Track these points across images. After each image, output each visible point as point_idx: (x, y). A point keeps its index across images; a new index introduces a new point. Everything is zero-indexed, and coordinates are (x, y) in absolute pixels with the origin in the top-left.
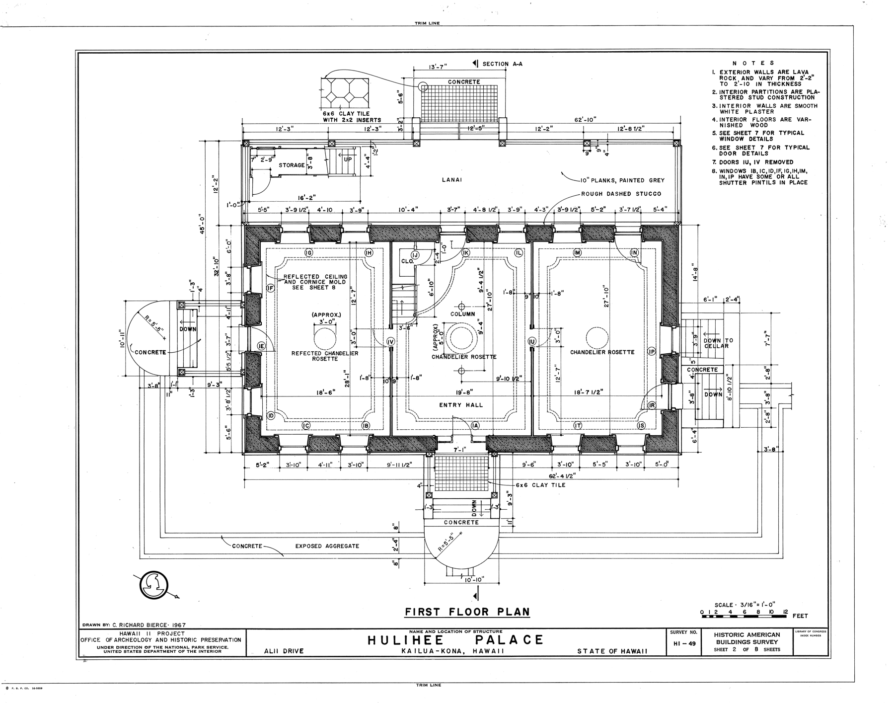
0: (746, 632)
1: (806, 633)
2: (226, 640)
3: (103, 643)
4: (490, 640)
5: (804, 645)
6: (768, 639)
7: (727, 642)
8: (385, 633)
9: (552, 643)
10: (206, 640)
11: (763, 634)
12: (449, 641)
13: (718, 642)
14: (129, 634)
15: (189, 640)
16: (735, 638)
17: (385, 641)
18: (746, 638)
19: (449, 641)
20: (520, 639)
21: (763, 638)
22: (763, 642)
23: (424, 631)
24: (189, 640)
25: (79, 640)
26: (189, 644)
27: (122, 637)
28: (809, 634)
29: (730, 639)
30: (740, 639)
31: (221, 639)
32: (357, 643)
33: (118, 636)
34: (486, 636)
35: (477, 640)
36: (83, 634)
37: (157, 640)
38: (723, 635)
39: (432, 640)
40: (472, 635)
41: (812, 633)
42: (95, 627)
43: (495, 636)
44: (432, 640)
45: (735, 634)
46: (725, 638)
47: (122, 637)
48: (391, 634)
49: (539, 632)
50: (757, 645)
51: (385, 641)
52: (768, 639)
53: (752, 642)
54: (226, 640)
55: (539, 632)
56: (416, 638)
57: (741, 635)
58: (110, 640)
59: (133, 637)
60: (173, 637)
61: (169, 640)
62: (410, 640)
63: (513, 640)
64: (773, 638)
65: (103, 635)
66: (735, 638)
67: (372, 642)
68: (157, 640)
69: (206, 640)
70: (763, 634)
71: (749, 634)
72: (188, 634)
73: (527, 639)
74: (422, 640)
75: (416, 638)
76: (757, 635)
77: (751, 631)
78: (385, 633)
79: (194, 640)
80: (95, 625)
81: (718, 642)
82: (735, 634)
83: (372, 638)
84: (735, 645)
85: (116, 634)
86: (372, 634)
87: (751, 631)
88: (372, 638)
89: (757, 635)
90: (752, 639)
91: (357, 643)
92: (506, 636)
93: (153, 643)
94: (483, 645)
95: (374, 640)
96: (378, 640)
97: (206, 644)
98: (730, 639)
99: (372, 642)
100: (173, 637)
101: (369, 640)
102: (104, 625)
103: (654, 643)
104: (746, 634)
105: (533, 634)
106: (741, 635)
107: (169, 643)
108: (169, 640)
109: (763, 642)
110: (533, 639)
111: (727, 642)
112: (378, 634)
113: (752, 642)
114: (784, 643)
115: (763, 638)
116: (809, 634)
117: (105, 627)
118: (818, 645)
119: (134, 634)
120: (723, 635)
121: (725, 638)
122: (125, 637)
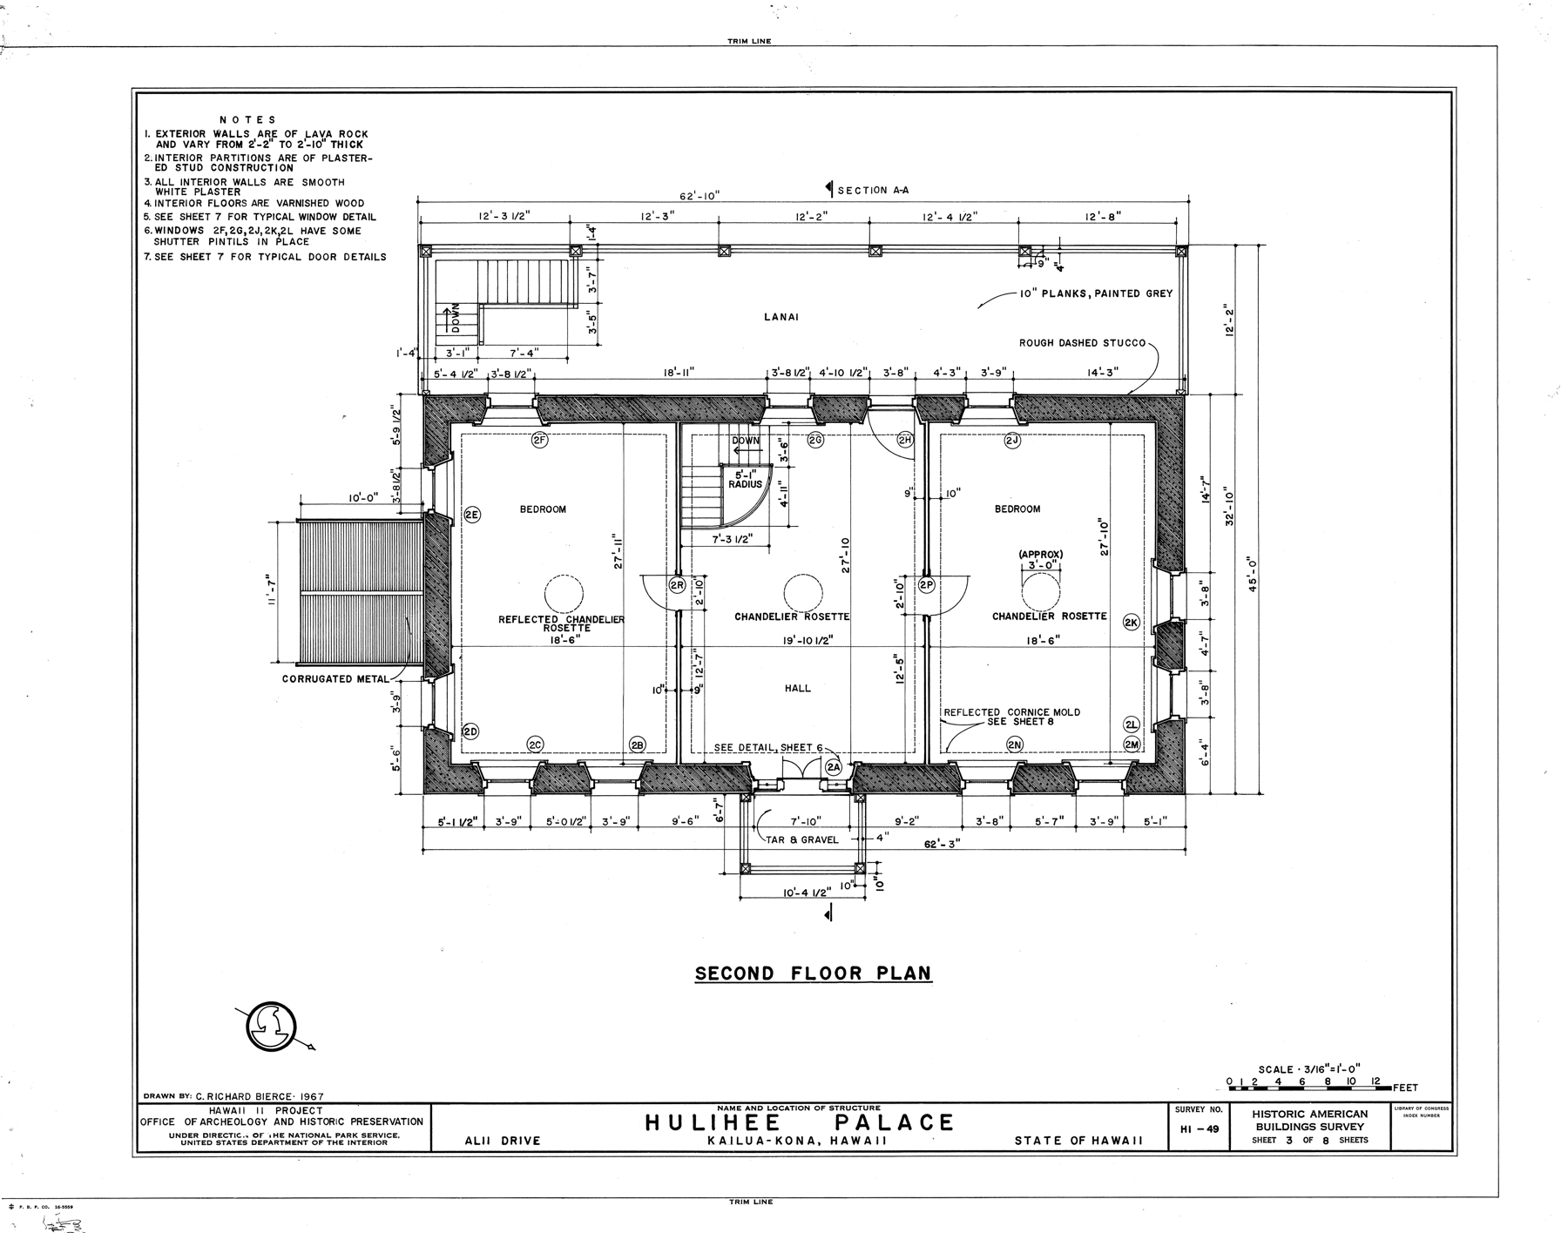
1: (1414, 1111)
2: (397, 1122)
3: (180, 1127)
4: (863, 1123)
5: (1410, 1131)
6: (1346, 1121)
7: (1274, 1127)
8: (676, 1110)
9: (970, 1128)
11: (1338, 1113)
12: (789, 1123)
14: (226, 1111)
15: (331, 1121)
16: (1289, 1120)
17: (676, 1124)
18: (1308, 1120)
20: (915, 1122)
23: (744, 1107)
24: (331, 1121)
25: (138, 1122)
26: (332, 1130)
27: (213, 1116)
28: (1419, 1113)
29: (1279, 1121)
30: (1298, 1121)
31: (386, 1121)
32: (627, 1129)
34: (854, 1117)
35: (838, 1123)
36: (145, 1112)
38: (1267, 1114)
39: (761, 1121)
40: (829, 1116)
41: (1423, 1111)
42: (166, 1099)
43: (872, 1117)
44: (761, 1121)
45: (1289, 1113)
46: (1271, 1120)
47: (213, 1116)
48: (687, 1112)
49: (946, 1109)
50: (1327, 1133)
51: (676, 1124)
52: (1346, 1121)
53: (1318, 1127)
54: (397, 1122)
55: (946, 1109)
56: (731, 1118)
57: (1298, 1114)
58: (193, 1121)
59: (234, 1116)
60: (302, 1116)
62: (720, 1122)
63: (905, 1123)
65: (180, 1113)
66: (1289, 1120)
67: (652, 1126)
68: (277, 1122)
70: (1338, 1113)
71: (1313, 1114)
72: (327, 1112)
73: (927, 1122)
74: (742, 1122)
75: (731, 1118)
76: (1328, 1114)
77: (1317, 1108)
78: (676, 1110)
79: (340, 1121)
80: (165, 1096)
82: (1289, 1113)
83: (652, 1118)
85: (203, 1112)
86: (652, 1111)
87: (1317, 1108)
88: (652, 1118)
89: (1328, 1114)
90: (1318, 1121)
91: (627, 1129)
92: (892, 1116)
93: (268, 1130)
94: (848, 1130)
95: (656, 1122)
96: (664, 1122)
97: (360, 1129)
98: (1279, 1121)
99: (652, 1126)
101: (648, 1122)
102: (182, 1096)
103: (1148, 1126)
104: (1308, 1113)
105: (936, 1111)
106: (1298, 1114)
107: (297, 1128)
109: (1338, 1126)
110: (936, 1122)
111: (1274, 1127)
112: (664, 1112)
113: (1318, 1127)
114: (1375, 1128)
116: (1419, 1113)
117: (184, 1100)
118: (1434, 1132)
120: (1267, 1114)
121: (1271, 1120)
122: (218, 1116)
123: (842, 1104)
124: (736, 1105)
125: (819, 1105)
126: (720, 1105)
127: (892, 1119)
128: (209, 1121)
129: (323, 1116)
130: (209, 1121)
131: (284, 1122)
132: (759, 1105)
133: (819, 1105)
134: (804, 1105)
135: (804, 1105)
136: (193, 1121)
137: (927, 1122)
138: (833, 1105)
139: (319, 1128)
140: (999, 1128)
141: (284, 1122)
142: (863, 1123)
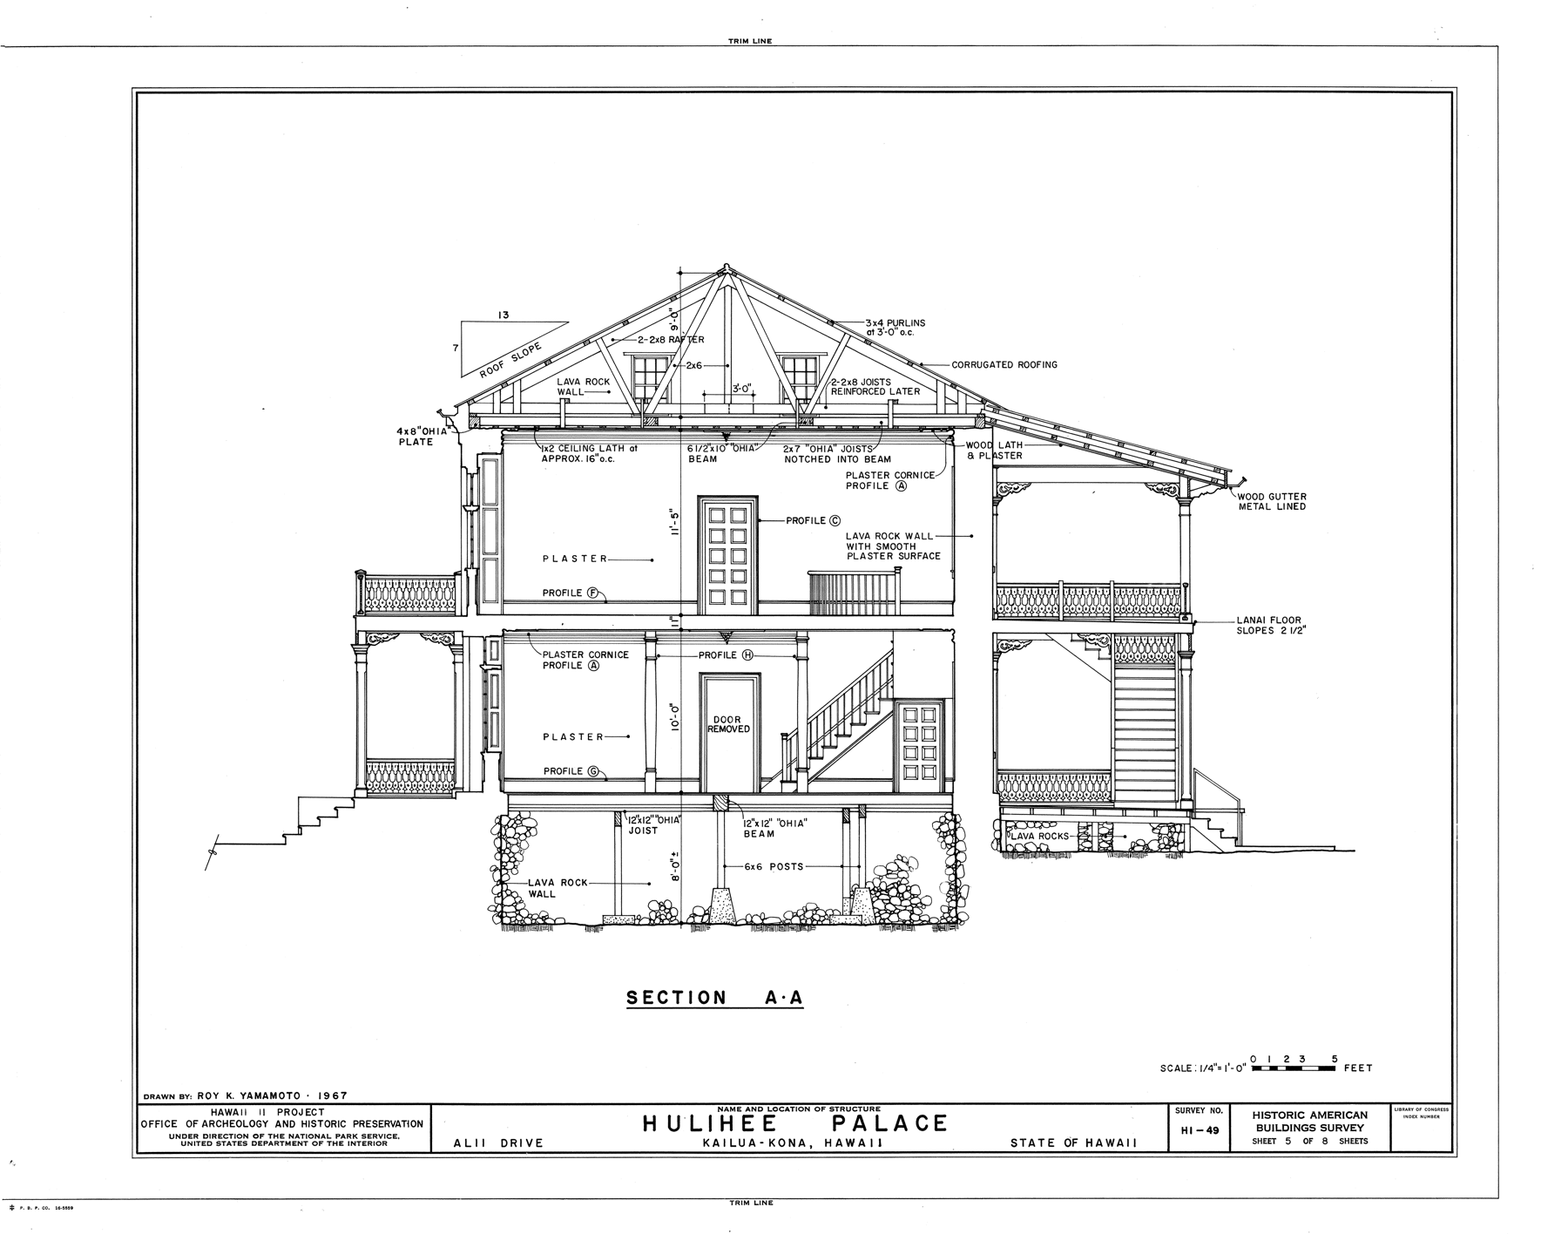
0: (1308, 1110)
1: (1414, 1113)
2: (397, 1124)
3: (182, 1129)
4: (860, 1124)
5: (1410, 1133)
6: (1346, 1122)
7: (1274, 1128)
8: (674, 1111)
10: (361, 1123)
11: (1338, 1114)
12: (786, 1125)
13: (1260, 1128)
14: (229, 1113)
15: (333, 1123)
16: (1289, 1121)
17: (674, 1126)
18: (1308, 1121)
19: (786, 1125)
21: (1338, 1121)
22: (1338, 1127)
23: (744, 1108)
24: (333, 1123)
25: (137, 1124)
26: (332, 1131)
27: (215, 1118)
28: (1419, 1114)
29: (1279, 1122)
30: (1298, 1122)
31: (387, 1123)
32: (624, 1129)
33: (209, 1118)
34: (851, 1117)
35: (835, 1123)
36: (146, 1113)
37: (278, 1124)
38: (1267, 1115)
39: (757, 1121)
40: (828, 1115)
41: (1423, 1112)
42: (166, 1100)
43: (869, 1118)
44: (757, 1121)
45: (1289, 1115)
46: (1271, 1121)
47: (215, 1118)
48: (685, 1112)
50: (1327, 1134)
51: (674, 1126)
52: (1346, 1122)
53: (1318, 1128)
54: (397, 1124)
56: (727, 1119)
57: (1298, 1115)
58: (195, 1123)
59: (236, 1118)
60: (304, 1118)
61: (298, 1124)
63: (901, 1123)
64: (1356, 1121)
65: (182, 1114)
66: (1289, 1121)
67: (650, 1127)
68: (278, 1124)
69: (361, 1123)
70: (1338, 1114)
71: (1313, 1115)
72: (331, 1113)
74: (738, 1123)
75: (727, 1119)
76: (1328, 1115)
77: (1317, 1109)
78: (674, 1111)
79: (341, 1124)
80: (165, 1097)
81: (1260, 1128)
82: (1289, 1115)
83: (650, 1119)
84: (1288, 1134)
85: (204, 1113)
86: (650, 1112)
87: (1317, 1109)
88: (650, 1119)
89: (1328, 1115)
90: (1318, 1122)
91: (624, 1129)
92: (888, 1117)
93: (271, 1128)
94: (845, 1131)
95: (654, 1123)
96: (662, 1123)
97: (360, 1131)
98: (1279, 1122)
99: (650, 1127)
100: (304, 1118)
101: (646, 1123)
102: (182, 1097)
103: (1147, 1129)
104: (1308, 1114)
105: (931, 1112)
106: (1298, 1115)
107: (298, 1130)
108: (298, 1124)
109: (1338, 1127)
111: (1274, 1128)
113: (1318, 1128)
114: (1375, 1130)
115: (1338, 1121)
116: (1419, 1114)
117: (183, 1101)
118: (1434, 1133)
119: (236, 1113)
120: (1267, 1115)
121: (1271, 1121)
122: (221, 1118)
123: (842, 1105)
124: (736, 1106)
125: (820, 1106)
126: (721, 1106)
128: (212, 1123)
129: (324, 1118)
130: (212, 1123)
131: (286, 1124)
132: (758, 1106)
133: (820, 1106)
134: (804, 1106)
135: (804, 1106)
136: (195, 1123)
137: (922, 1123)
138: (833, 1105)
139: (319, 1130)
140: (997, 1129)
141: (286, 1124)
142: (860, 1124)
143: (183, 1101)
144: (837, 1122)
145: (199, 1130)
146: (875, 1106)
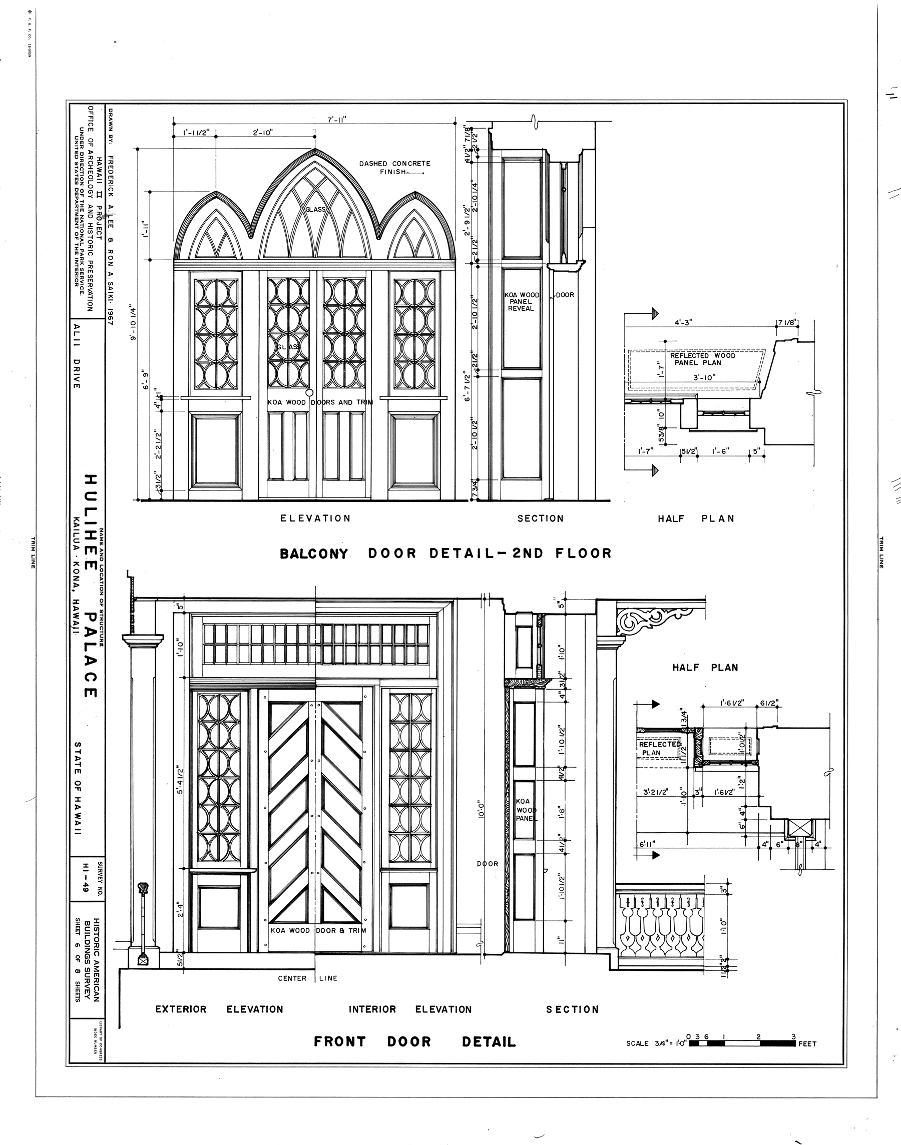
0: (100, 959)
2: (90, 293)
3: (87, 135)
4: (90, 632)
5: (84, 1033)
6: (92, 986)
7: (87, 934)
8: (100, 497)
9: (87, 710)
10: (91, 266)
12: (89, 578)
13: (87, 923)
14: (99, 170)
15: (91, 246)
16: (92, 945)
17: (89, 496)
18: (93, 958)
19: (89, 578)
20: (91, 668)
21: (92, 980)
22: (88, 981)
23: (103, 547)
24: (91, 246)
25: (91, 104)
26: (85, 246)
27: (95, 160)
28: (98, 1039)
29: (91, 938)
30: (92, 951)
31: (91, 285)
32: (87, 460)
33: (95, 155)
34: (95, 625)
35: (90, 614)
36: (99, 110)
37: (90, 206)
38: (97, 929)
39: (91, 556)
40: (97, 608)
41: (99, 1042)
42: (108, 125)
43: (95, 638)
44: (91, 556)
45: (97, 945)
46: (92, 932)
47: (95, 160)
48: (99, 504)
49: (100, 692)
50: (83, 972)
51: (89, 496)
52: (92, 986)
53: (87, 966)
54: (90, 293)
55: (100, 692)
56: (94, 535)
57: (97, 951)
58: (92, 144)
59: (95, 175)
60: (95, 226)
61: (90, 221)
62: (91, 528)
63: (91, 661)
64: (92, 993)
65: (98, 135)
66: (92, 945)
67: (88, 479)
68: (90, 206)
69: (91, 266)
70: (97, 980)
71: (97, 962)
72: (99, 245)
73: (91, 677)
74: (91, 543)
75: (94, 535)
76: (97, 973)
77: (101, 965)
78: (100, 497)
79: (91, 252)
80: (111, 124)
81: (87, 923)
82: (97, 945)
83: (94, 479)
84: (83, 944)
85: (98, 152)
86: (99, 479)
87: (101, 965)
88: (94, 479)
89: (97, 973)
90: (91, 966)
91: (87, 460)
92: (95, 652)
93: (88, 201)
94: (84, 621)
95: (91, 482)
96: (91, 488)
97: (85, 266)
98: (91, 938)
99: (88, 479)
100: (95, 226)
101: (91, 476)
102: (111, 136)
103: (88, 841)
104: (97, 958)
105: (98, 685)
106: (97, 951)
107: (87, 221)
108: (90, 221)
109: (88, 981)
110: (91, 685)
111: (87, 934)
112: (98, 487)
113: (87, 966)
114: (86, 1007)
115: (92, 980)
116: (98, 1039)
117: (108, 138)
118: (83, 1050)
119: (99, 175)
120: (97, 929)
121: (92, 932)
122: (95, 163)
123: (104, 619)
124: (104, 542)
125: (104, 603)
126: (104, 531)
127: (92, 652)
128: (91, 157)
129: (94, 239)
130: (91, 157)
131: (90, 212)
132: (104, 558)
133: (104, 603)
134: (103, 591)
135: (103, 591)
136: (92, 144)
137: (91, 677)
138: (104, 612)
139: (86, 236)
140: (87, 730)
141: (90, 212)
142: (90, 632)
143: (108, 138)
144: (91, 615)
145: (87, 147)
146: (103, 643)
